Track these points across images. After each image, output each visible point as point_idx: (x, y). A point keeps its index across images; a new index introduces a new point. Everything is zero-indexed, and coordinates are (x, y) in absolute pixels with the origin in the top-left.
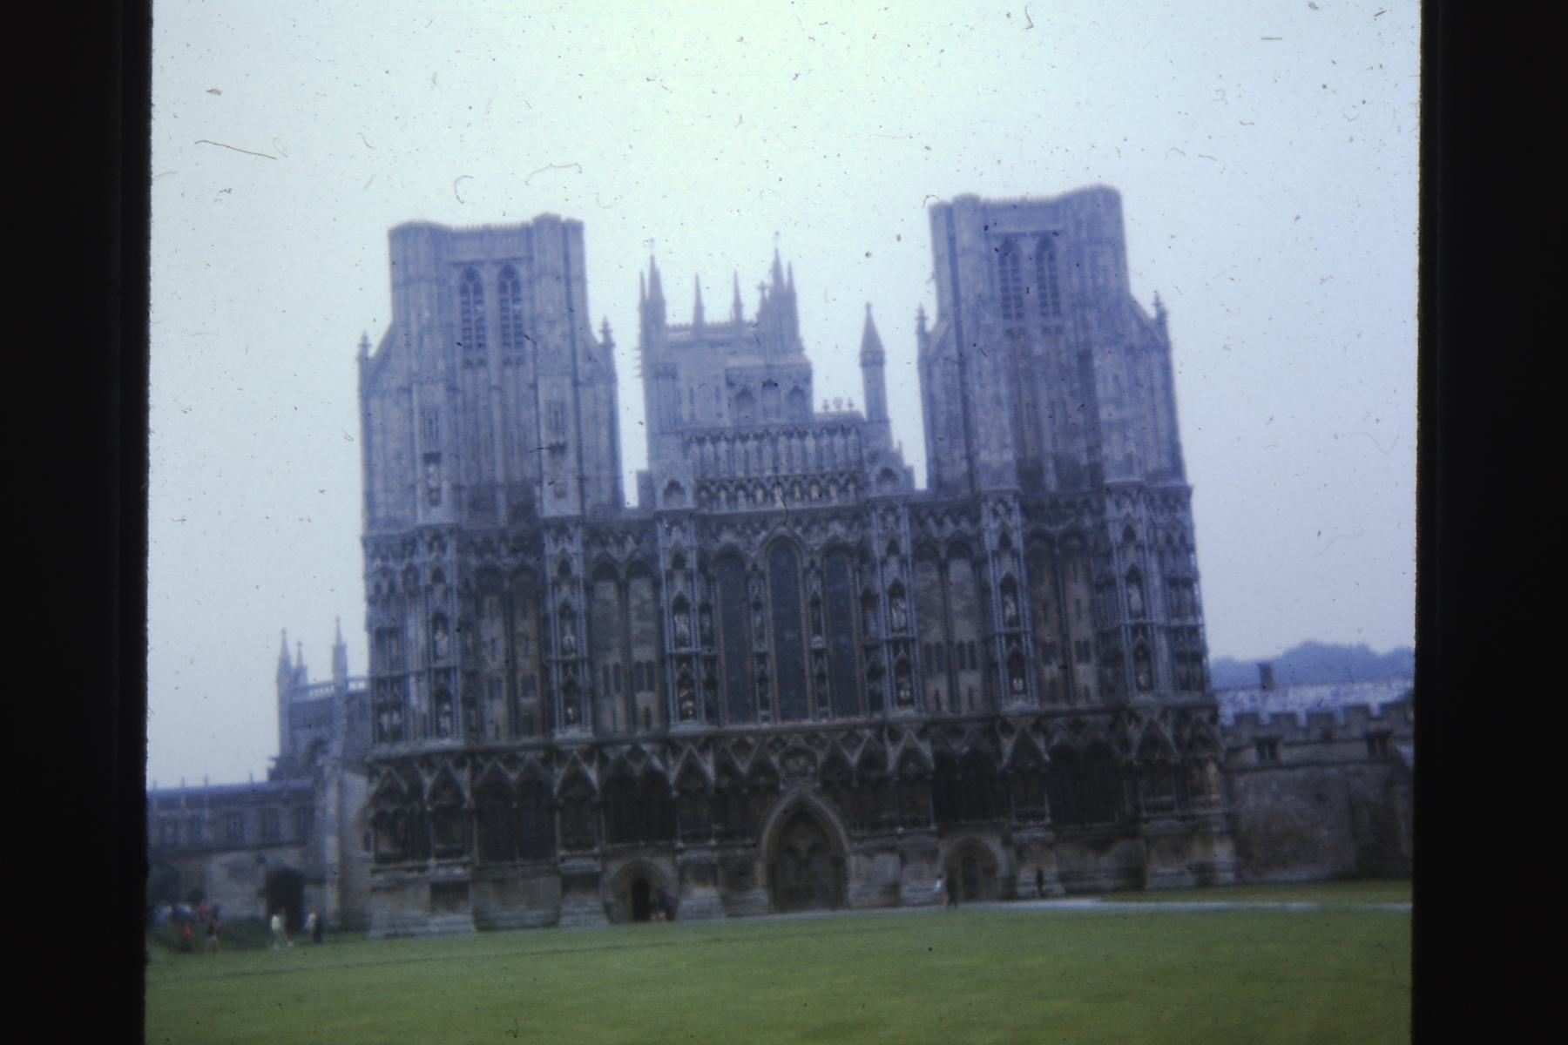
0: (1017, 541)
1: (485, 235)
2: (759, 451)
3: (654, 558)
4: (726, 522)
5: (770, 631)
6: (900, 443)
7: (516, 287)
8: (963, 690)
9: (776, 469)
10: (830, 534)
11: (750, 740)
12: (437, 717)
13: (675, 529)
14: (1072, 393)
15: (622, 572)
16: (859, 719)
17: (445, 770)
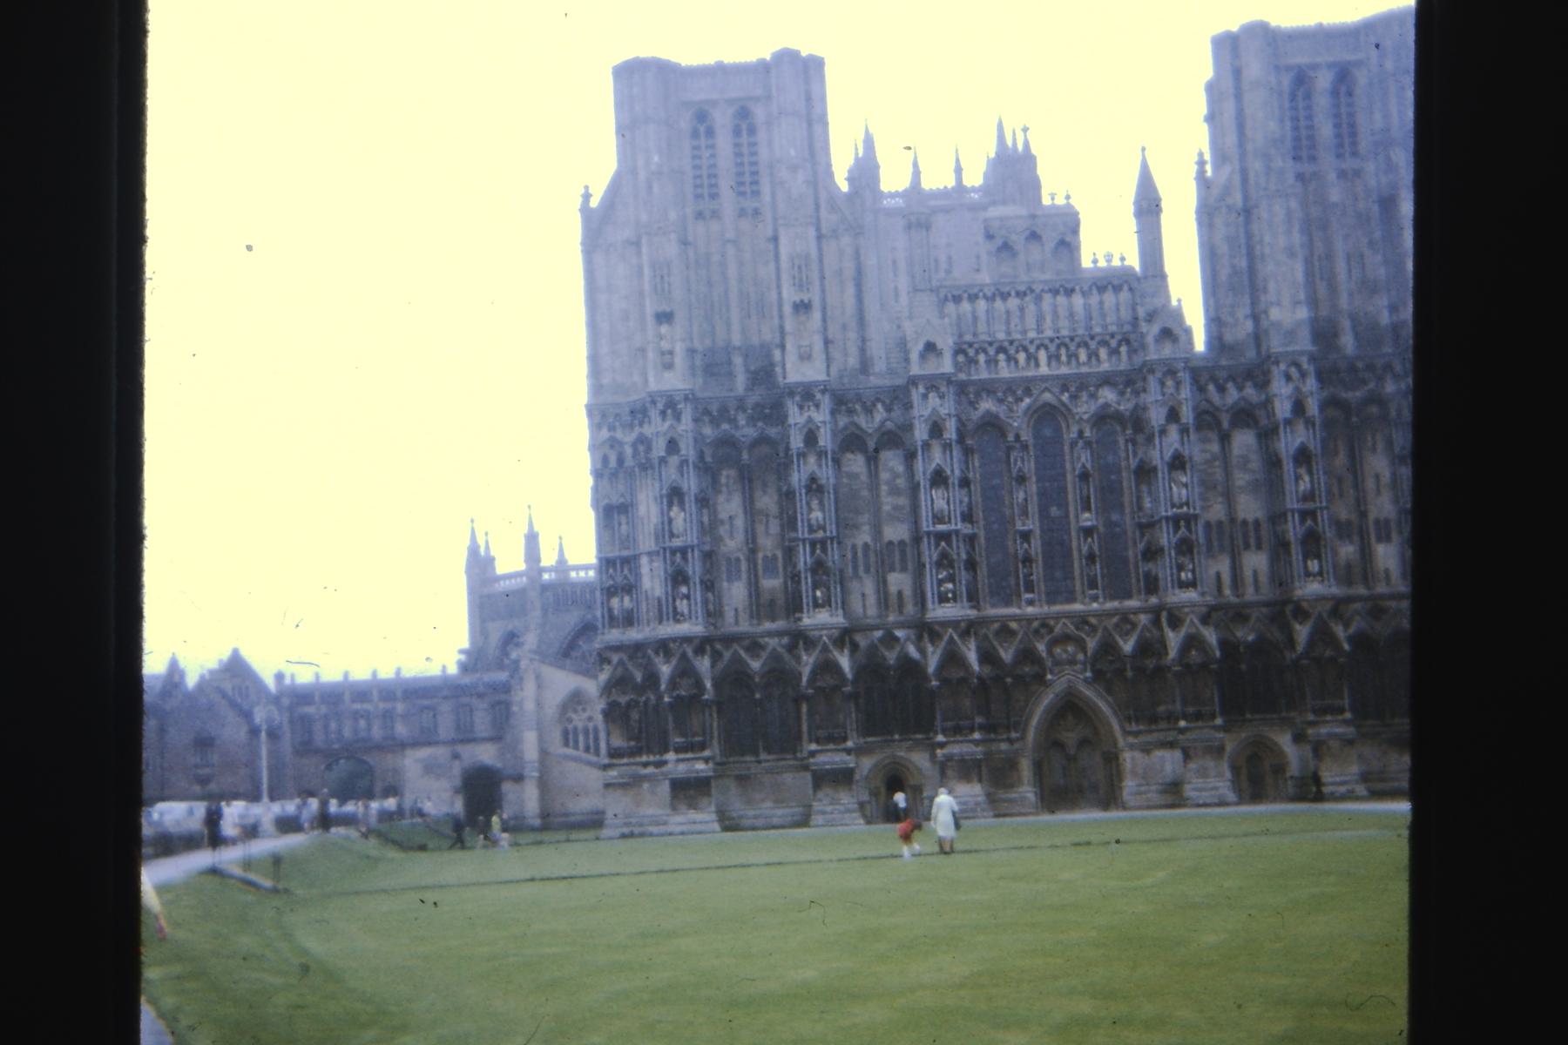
0: (1312, 407)
1: (721, 71)
2: (1022, 309)
3: (908, 427)
4: (986, 388)
5: (1033, 508)
6: (1179, 301)
7: (752, 131)
8: (1248, 574)
9: (1040, 330)
10: (1101, 401)
11: (1014, 625)
12: (674, 600)
13: (931, 395)
14: (1371, 243)
15: (871, 444)
16: (1133, 603)
17: (684, 656)
